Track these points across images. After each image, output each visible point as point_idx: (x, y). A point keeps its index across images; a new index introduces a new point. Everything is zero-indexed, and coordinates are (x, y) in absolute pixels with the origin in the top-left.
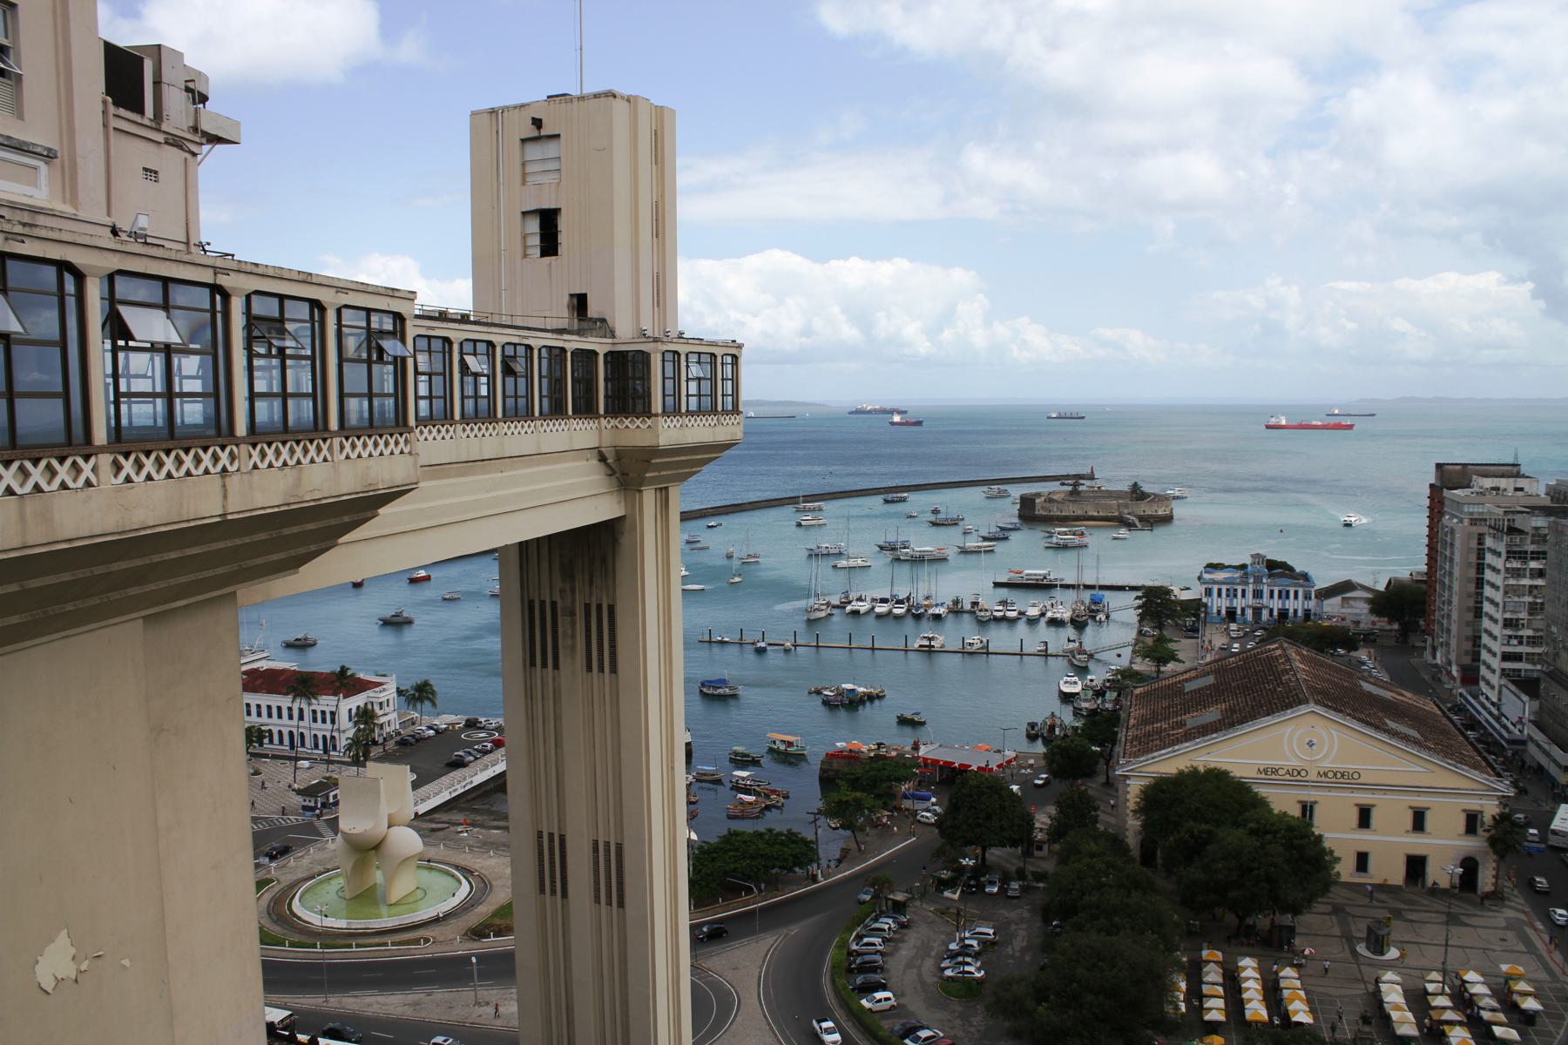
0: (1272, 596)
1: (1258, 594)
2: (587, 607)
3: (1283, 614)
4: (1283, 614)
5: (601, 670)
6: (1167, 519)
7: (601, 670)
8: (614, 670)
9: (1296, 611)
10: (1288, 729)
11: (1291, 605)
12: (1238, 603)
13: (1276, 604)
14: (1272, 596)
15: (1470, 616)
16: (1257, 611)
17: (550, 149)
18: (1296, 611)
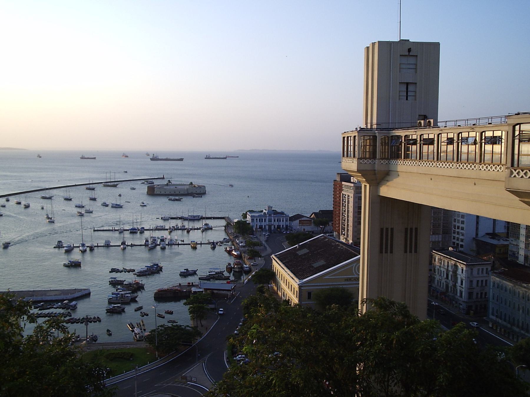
0: (275, 221)
1: (270, 221)
2: (406, 230)
3: (279, 227)
4: (279, 227)
5: (411, 252)
6: (204, 193)
7: (411, 252)
8: (416, 251)
9: (283, 226)
10: (355, 265)
11: (281, 224)
12: (263, 224)
13: (276, 224)
14: (275, 221)
15: (356, 224)
16: (270, 226)
17: (412, 60)
18: (283, 226)
